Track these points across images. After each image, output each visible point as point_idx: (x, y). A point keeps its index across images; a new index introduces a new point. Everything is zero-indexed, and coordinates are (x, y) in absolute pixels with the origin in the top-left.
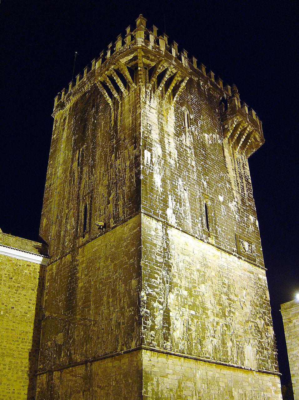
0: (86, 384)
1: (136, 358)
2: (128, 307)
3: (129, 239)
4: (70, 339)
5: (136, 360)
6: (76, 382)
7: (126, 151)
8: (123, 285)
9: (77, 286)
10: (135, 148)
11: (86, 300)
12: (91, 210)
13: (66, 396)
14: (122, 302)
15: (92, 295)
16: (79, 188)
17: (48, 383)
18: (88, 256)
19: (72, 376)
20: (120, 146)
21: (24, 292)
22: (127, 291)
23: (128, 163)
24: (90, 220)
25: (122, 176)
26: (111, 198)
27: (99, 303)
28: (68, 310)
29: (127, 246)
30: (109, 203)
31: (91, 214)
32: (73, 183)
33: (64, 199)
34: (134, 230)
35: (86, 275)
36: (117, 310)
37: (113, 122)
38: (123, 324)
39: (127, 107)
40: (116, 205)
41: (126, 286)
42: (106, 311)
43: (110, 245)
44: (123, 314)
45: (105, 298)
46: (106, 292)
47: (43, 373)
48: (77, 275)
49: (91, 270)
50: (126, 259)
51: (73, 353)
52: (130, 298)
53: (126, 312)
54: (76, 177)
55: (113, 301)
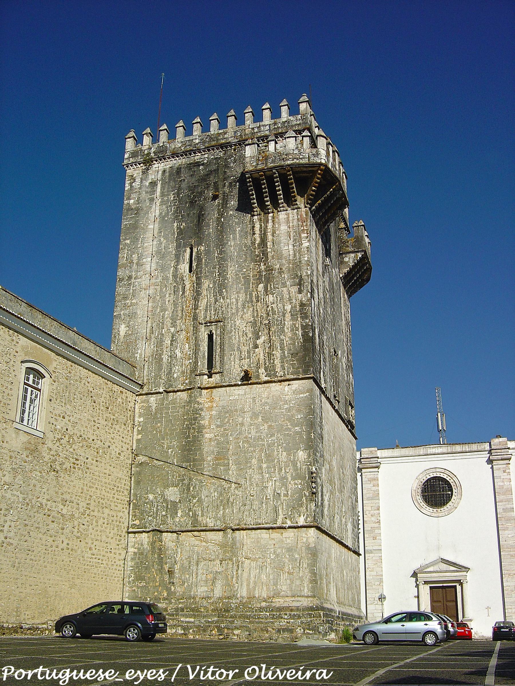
0: (225, 552)
1: (306, 534)
2: (293, 479)
3: (293, 402)
4: (194, 497)
5: (306, 536)
6: (207, 548)
7: (285, 289)
8: (285, 454)
9: (203, 436)
10: (300, 292)
11: (221, 456)
12: (222, 345)
13: (190, 562)
14: (283, 471)
15: (230, 452)
16: (196, 307)
17: (153, 544)
18: (221, 403)
19: (201, 541)
20: (274, 278)
21: (117, 427)
22: (290, 460)
23: (288, 307)
24: (222, 357)
25: (277, 320)
26: (259, 342)
27: (243, 465)
28: (187, 461)
29: (289, 410)
30: (256, 346)
31: (222, 350)
32: (181, 293)
33: (164, 310)
34: (300, 394)
35: (218, 426)
36: (275, 479)
37: (257, 236)
38: (286, 495)
39: (284, 228)
40: (270, 355)
41: (289, 454)
42: (257, 477)
43: (261, 401)
44: (284, 485)
45: (254, 461)
46: (256, 455)
47: (141, 532)
48: (202, 422)
49: (227, 422)
50: (289, 424)
51: (200, 515)
52: (296, 469)
53: (290, 483)
54: (188, 287)
55: (267, 467)
